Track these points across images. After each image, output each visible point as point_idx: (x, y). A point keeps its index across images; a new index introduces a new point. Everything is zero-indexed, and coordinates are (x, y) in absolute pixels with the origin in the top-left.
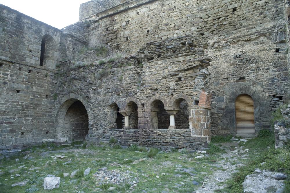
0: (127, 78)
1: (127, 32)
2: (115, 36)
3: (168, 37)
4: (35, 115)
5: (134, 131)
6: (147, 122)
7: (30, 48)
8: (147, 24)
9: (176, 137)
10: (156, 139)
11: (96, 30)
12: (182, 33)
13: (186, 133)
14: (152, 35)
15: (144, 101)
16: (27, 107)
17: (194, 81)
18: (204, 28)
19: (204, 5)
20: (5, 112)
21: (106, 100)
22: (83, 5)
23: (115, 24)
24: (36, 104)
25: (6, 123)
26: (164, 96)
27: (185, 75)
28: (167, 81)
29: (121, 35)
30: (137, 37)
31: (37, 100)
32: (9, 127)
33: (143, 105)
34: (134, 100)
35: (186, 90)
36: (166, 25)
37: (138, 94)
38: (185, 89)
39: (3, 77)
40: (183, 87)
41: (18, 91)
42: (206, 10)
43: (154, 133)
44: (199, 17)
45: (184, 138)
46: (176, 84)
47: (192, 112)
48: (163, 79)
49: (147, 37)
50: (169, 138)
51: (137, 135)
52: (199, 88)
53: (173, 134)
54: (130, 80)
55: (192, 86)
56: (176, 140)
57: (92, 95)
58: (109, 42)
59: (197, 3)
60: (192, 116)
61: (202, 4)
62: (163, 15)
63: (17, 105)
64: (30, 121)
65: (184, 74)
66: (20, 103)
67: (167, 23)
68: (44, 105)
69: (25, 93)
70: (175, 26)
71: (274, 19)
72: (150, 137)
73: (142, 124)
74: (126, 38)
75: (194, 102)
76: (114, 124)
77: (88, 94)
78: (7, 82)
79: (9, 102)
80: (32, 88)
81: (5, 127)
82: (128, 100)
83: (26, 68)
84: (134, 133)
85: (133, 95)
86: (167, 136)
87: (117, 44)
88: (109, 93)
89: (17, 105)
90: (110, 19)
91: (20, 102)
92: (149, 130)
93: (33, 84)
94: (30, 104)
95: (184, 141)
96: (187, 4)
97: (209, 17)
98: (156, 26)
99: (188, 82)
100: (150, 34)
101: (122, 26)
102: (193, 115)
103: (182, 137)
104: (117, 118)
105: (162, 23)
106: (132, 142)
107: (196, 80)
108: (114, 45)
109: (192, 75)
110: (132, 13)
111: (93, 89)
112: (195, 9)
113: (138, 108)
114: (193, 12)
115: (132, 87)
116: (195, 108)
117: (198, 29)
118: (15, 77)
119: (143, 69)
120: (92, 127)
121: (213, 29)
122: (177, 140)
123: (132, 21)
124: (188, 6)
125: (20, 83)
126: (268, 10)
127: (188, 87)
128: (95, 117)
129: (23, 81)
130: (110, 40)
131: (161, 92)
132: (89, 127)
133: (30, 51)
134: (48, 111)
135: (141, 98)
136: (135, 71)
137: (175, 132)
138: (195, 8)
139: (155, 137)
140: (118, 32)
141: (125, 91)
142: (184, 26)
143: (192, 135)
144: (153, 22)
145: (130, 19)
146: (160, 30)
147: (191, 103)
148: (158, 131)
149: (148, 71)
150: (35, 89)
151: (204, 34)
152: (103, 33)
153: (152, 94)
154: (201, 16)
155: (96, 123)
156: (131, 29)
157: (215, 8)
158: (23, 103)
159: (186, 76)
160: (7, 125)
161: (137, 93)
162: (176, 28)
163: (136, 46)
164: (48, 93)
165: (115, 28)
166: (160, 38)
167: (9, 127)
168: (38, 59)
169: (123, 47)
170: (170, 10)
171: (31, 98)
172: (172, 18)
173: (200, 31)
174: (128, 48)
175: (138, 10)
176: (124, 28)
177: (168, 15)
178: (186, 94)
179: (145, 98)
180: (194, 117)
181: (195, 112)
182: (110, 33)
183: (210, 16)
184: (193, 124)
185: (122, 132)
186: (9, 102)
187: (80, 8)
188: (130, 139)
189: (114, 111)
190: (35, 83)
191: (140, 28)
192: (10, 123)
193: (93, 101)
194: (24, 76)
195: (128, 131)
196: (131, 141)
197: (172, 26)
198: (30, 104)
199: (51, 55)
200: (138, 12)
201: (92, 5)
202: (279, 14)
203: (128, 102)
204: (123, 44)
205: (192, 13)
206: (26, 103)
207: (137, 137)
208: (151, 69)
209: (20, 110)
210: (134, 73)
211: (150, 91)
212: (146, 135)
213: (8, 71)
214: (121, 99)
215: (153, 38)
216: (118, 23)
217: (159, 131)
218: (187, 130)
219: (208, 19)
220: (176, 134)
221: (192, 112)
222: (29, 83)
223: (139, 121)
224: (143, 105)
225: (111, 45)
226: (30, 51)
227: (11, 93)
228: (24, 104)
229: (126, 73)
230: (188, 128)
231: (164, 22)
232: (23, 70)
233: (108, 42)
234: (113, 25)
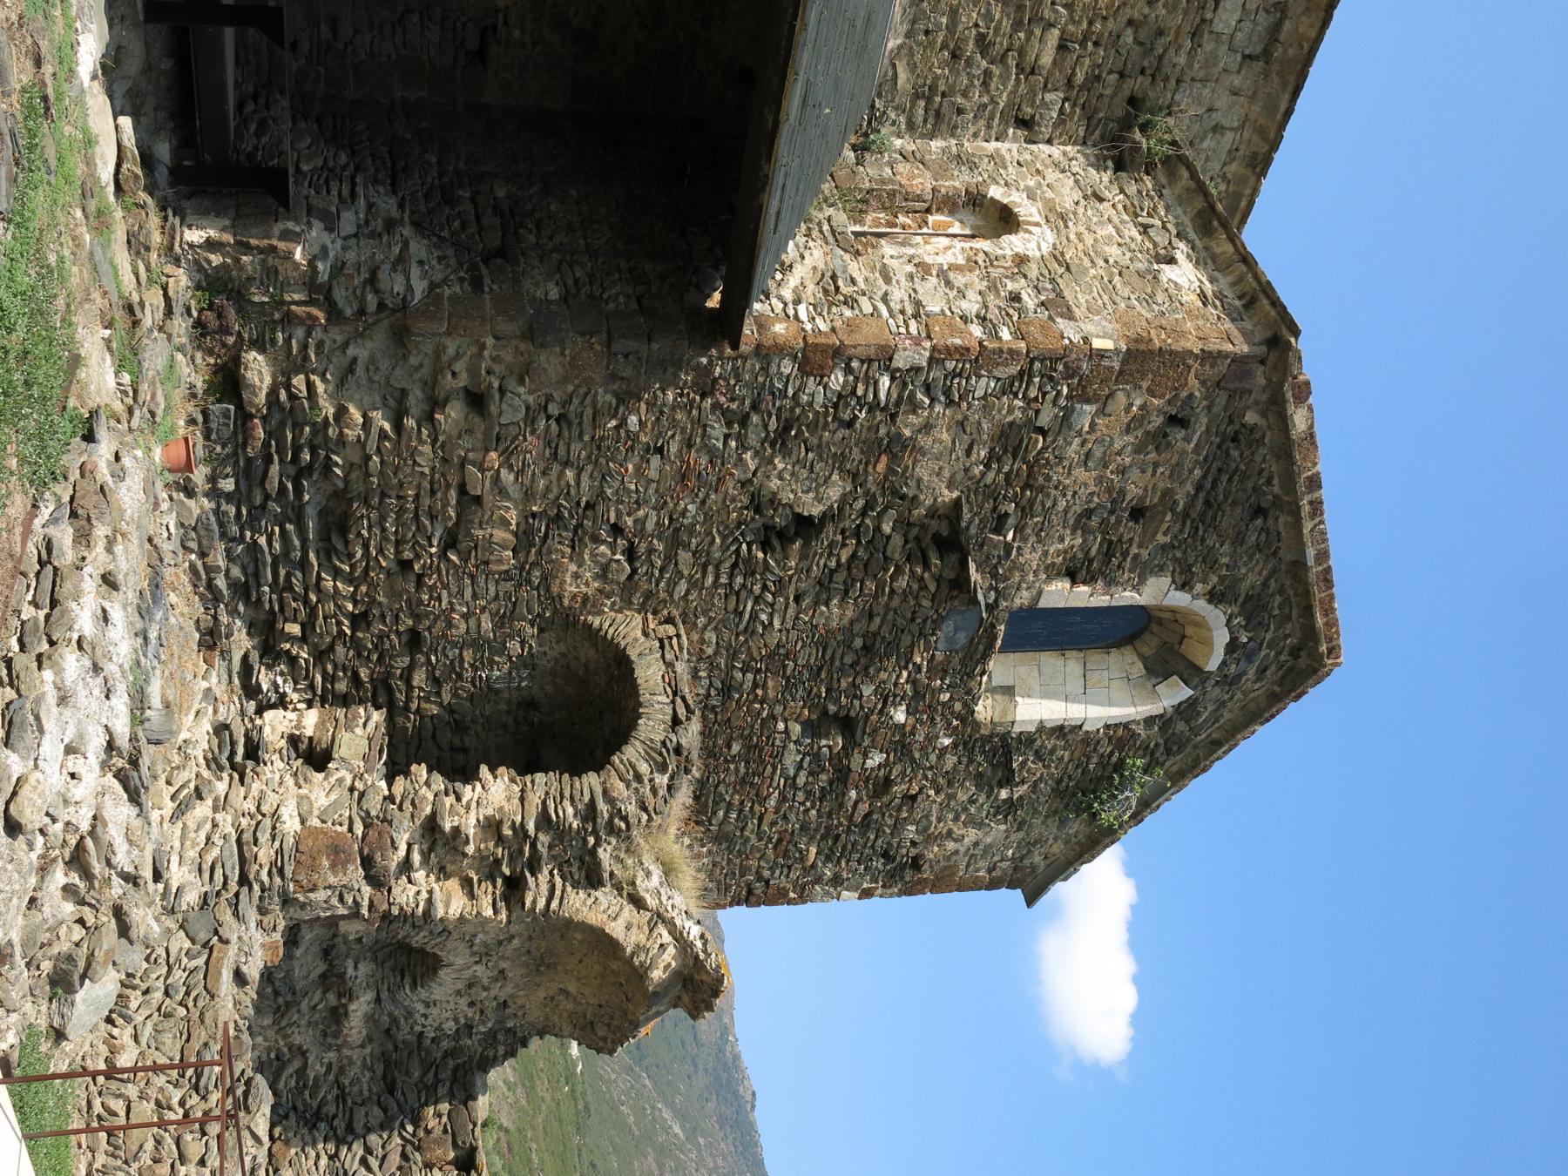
71: (917, 96)
126: (987, 74)
202: (938, 114)
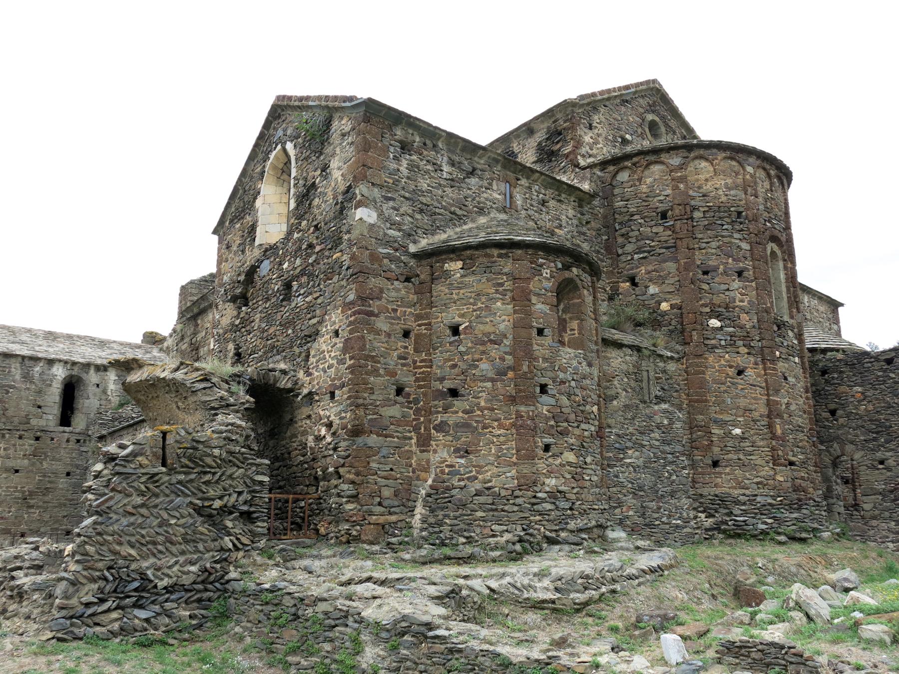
4: (45, 505)
16: (31, 493)
31: (50, 482)
41: (17, 471)
63: (15, 492)
68: (62, 489)
69: (28, 472)
80: (41, 463)
89: (15, 492)
118: (11, 452)
129: (25, 455)
133: (39, 407)
150: (45, 465)
190: (47, 456)
209: (19, 498)
226: (39, 407)
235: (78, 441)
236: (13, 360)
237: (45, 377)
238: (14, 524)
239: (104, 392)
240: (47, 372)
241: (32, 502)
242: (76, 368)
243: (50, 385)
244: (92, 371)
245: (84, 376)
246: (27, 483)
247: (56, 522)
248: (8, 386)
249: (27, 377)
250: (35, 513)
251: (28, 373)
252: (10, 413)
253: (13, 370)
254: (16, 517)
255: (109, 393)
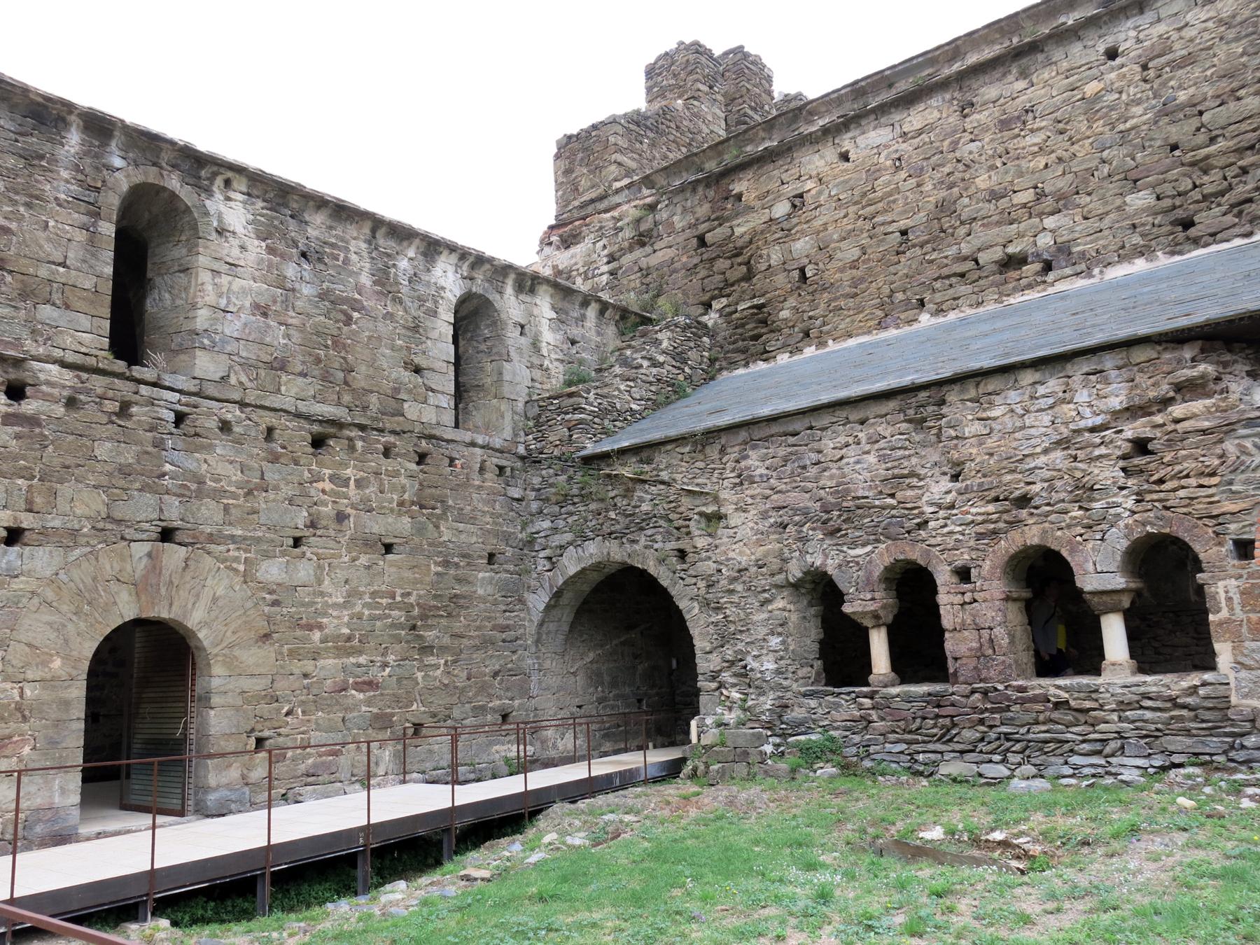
0: (872, 459)
1: (802, 246)
2: (744, 269)
3: (1011, 250)
5: (930, 694)
6: (990, 652)
7: (417, 360)
8: (894, 201)
9: (1148, 715)
10: (1044, 728)
11: (648, 249)
12: (1077, 228)
13: (1202, 692)
14: (928, 247)
15: (966, 557)
17: (1219, 451)
18: (1196, 195)
19: (1181, 87)
20: (349, 639)
21: (775, 564)
22: (567, 144)
23: (737, 215)
24: (456, 596)
25: (359, 687)
26: (1069, 526)
27: (1170, 428)
28: (1075, 458)
29: (772, 262)
30: (854, 265)
31: (459, 580)
32: (369, 702)
33: (963, 574)
34: (915, 554)
35: (1182, 493)
36: (994, 196)
37: (932, 524)
38: (1174, 490)
39: (333, 493)
40: (1161, 481)
41: (388, 548)
42: (1196, 108)
43: (1035, 700)
44: (1159, 143)
45: (1196, 716)
46: (1123, 469)
47: (1222, 596)
48: (1055, 449)
49: (903, 260)
50: (1115, 717)
51: (944, 711)
52: (1247, 482)
53: (1136, 698)
54: (884, 466)
55: (1213, 474)
56: (1153, 727)
57: (701, 542)
58: (714, 298)
59: (1145, 81)
60: (1224, 613)
61: (1172, 83)
62: (971, 153)
63: (390, 607)
64: (439, 672)
65: (1159, 419)
66: (398, 599)
67: (996, 188)
68: (483, 600)
70: (1041, 195)
72: (1012, 719)
73: (964, 661)
74: (796, 274)
75: (1229, 545)
76: (812, 666)
77: (678, 539)
78: (349, 510)
79: (360, 595)
80: (437, 527)
81: (355, 707)
82: (882, 556)
83: (400, 444)
84: (928, 703)
85: (909, 532)
86: (1101, 708)
87: (756, 301)
88: (785, 527)
89: (390, 607)
90: (712, 193)
91: (399, 592)
92: (1006, 687)
93: (438, 511)
94: (435, 597)
95: (1194, 732)
96: (1091, 88)
97: (1213, 140)
98: (941, 206)
99: (1186, 458)
100: (914, 246)
101: (771, 220)
102: (1232, 609)
103: (1184, 712)
104: (822, 636)
105: (972, 190)
106: (924, 742)
107: (1230, 446)
108: (740, 308)
109: (1206, 424)
110: (819, 161)
111: (701, 514)
112: (1137, 110)
113: (941, 589)
114: (1128, 125)
115: (899, 495)
116: (1241, 576)
117: (1158, 198)
118: (371, 490)
119: (945, 410)
120: (714, 685)
121: (1241, 191)
122: (1159, 726)
123: (820, 193)
124: (1097, 97)
125: (392, 510)
127: (1193, 481)
128: (724, 640)
130: (721, 285)
131: (1048, 508)
132: (699, 684)
133: (418, 370)
134: (501, 621)
135: (950, 542)
136: (905, 421)
137: (1142, 689)
138: (1138, 102)
139: (1041, 717)
140: (753, 246)
141: (865, 517)
142: (1089, 194)
143: (1234, 700)
144: (928, 187)
145: (809, 185)
146: (962, 223)
147: (1212, 552)
148: (1055, 687)
149: (970, 417)
151: (1196, 219)
152: (684, 259)
153: (1006, 522)
154: (1172, 141)
155: (732, 663)
156: (818, 233)
157: (1242, 92)
158: (409, 594)
159: (1175, 431)
160: (361, 696)
161: (926, 522)
162: (1049, 203)
163: (851, 303)
164: (493, 544)
165: (738, 231)
166: (965, 259)
167: (369, 702)
168: (446, 401)
169: (785, 314)
170: (1005, 124)
171: (437, 574)
172: (1023, 163)
173: (1174, 208)
174: (810, 318)
175: (846, 143)
176: (784, 230)
177: (1000, 149)
178: (1185, 510)
179: (972, 543)
180: (1239, 614)
181: (1242, 593)
182: (719, 256)
183: (1217, 136)
184: (1234, 648)
185: (867, 702)
186: (360, 595)
187: (558, 157)
188: (910, 732)
189: (810, 605)
190: (446, 509)
191: (860, 222)
192: (371, 685)
193: (709, 567)
194: (403, 480)
195: (898, 696)
196: (919, 738)
197: (1026, 196)
198: (435, 597)
199: (489, 380)
200: (847, 152)
201: (612, 139)
203: (888, 560)
204: (785, 300)
205: (1122, 127)
206: (420, 596)
207: (947, 721)
208: (985, 410)
210: (901, 434)
211: (991, 508)
212: (992, 711)
213: (347, 466)
214: (850, 551)
215: (932, 262)
216: (751, 209)
217: (1059, 687)
218: (1208, 676)
219: (1212, 148)
220: (1150, 698)
221: (1222, 596)
222: (422, 507)
223: (948, 646)
224: (963, 574)
225: (727, 310)
226: (418, 370)
227: (364, 560)
228: (412, 599)
229: (860, 435)
230: (1212, 667)
231: (983, 181)
232: (397, 455)
233: (709, 295)
234: (728, 219)
235: (501, 469)
236: (352, 230)
237: (422, 289)
238: (397, 699)
239: (535, 345)
240: (425, 277)
241: (430, 635)
242: (479, 276)
243: (434, 313)
244: (509, 290)
245: (493, 296)
246: (416, 581)
247: (483, 688)
248: (346, 300)
249: (383, 278)
250: (437, 667)
251: (388, 274)
252: (360, 378)
253: (354, 257)
254: (399, 680)
255: (545, 352)
